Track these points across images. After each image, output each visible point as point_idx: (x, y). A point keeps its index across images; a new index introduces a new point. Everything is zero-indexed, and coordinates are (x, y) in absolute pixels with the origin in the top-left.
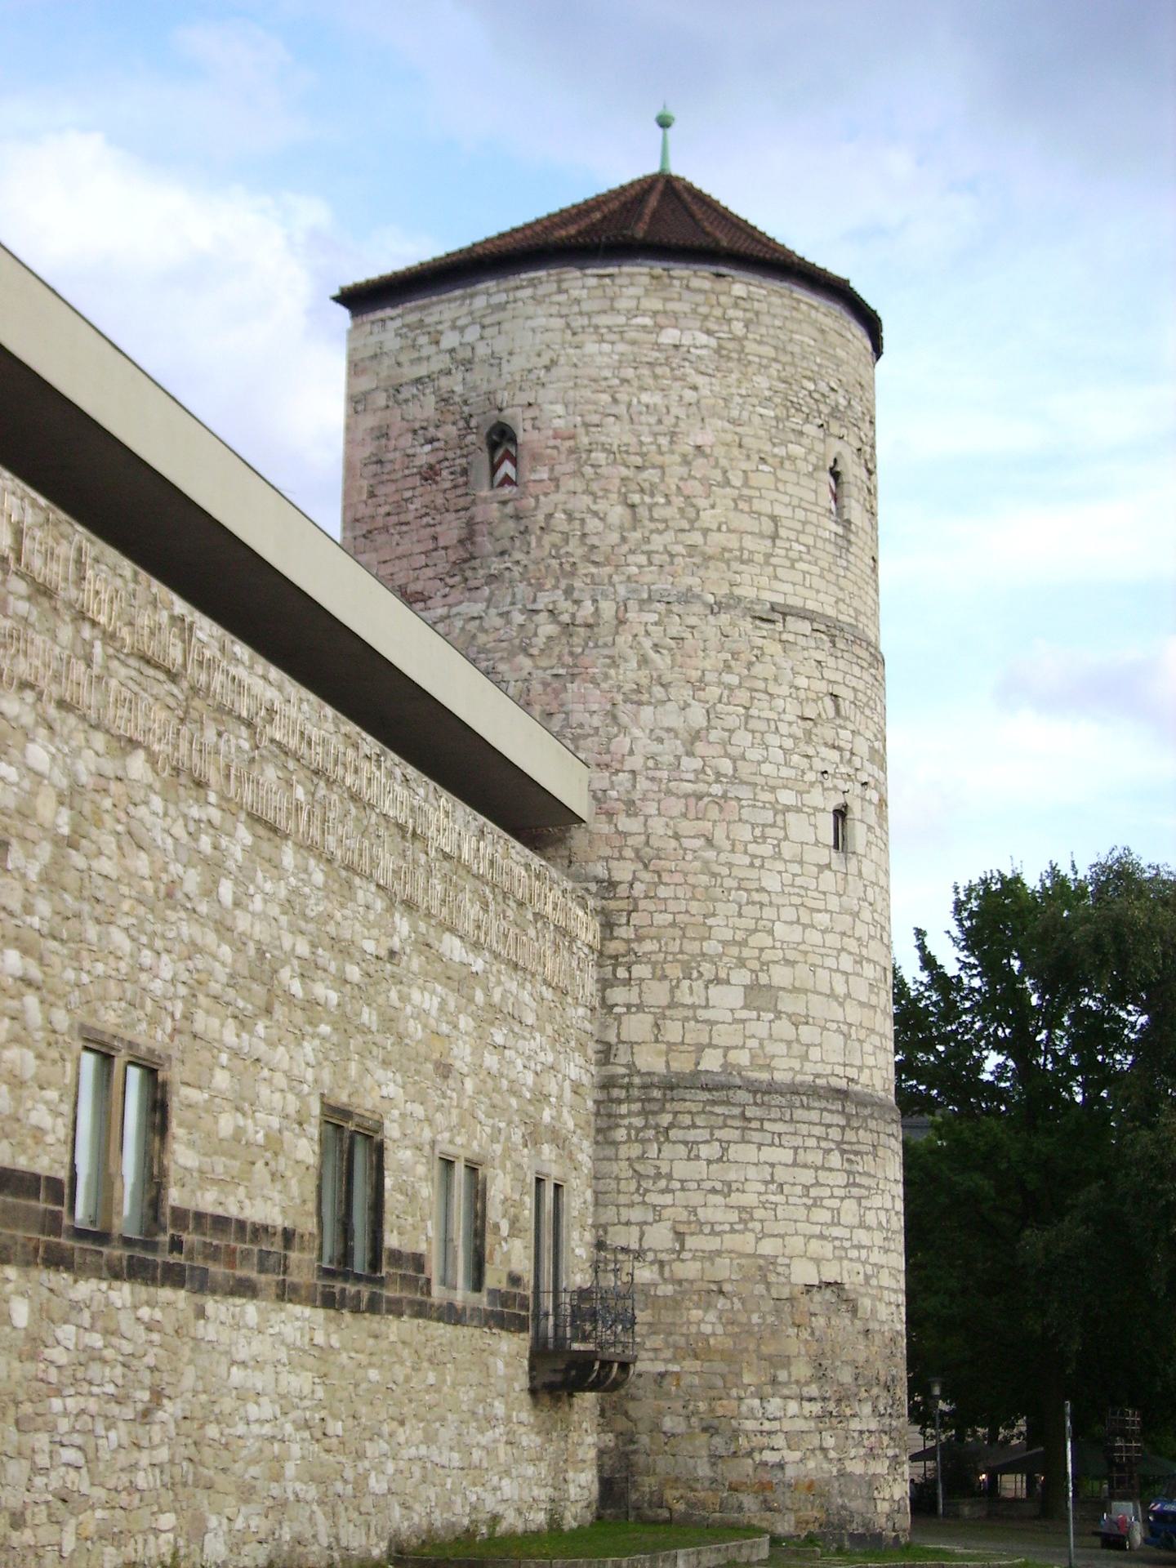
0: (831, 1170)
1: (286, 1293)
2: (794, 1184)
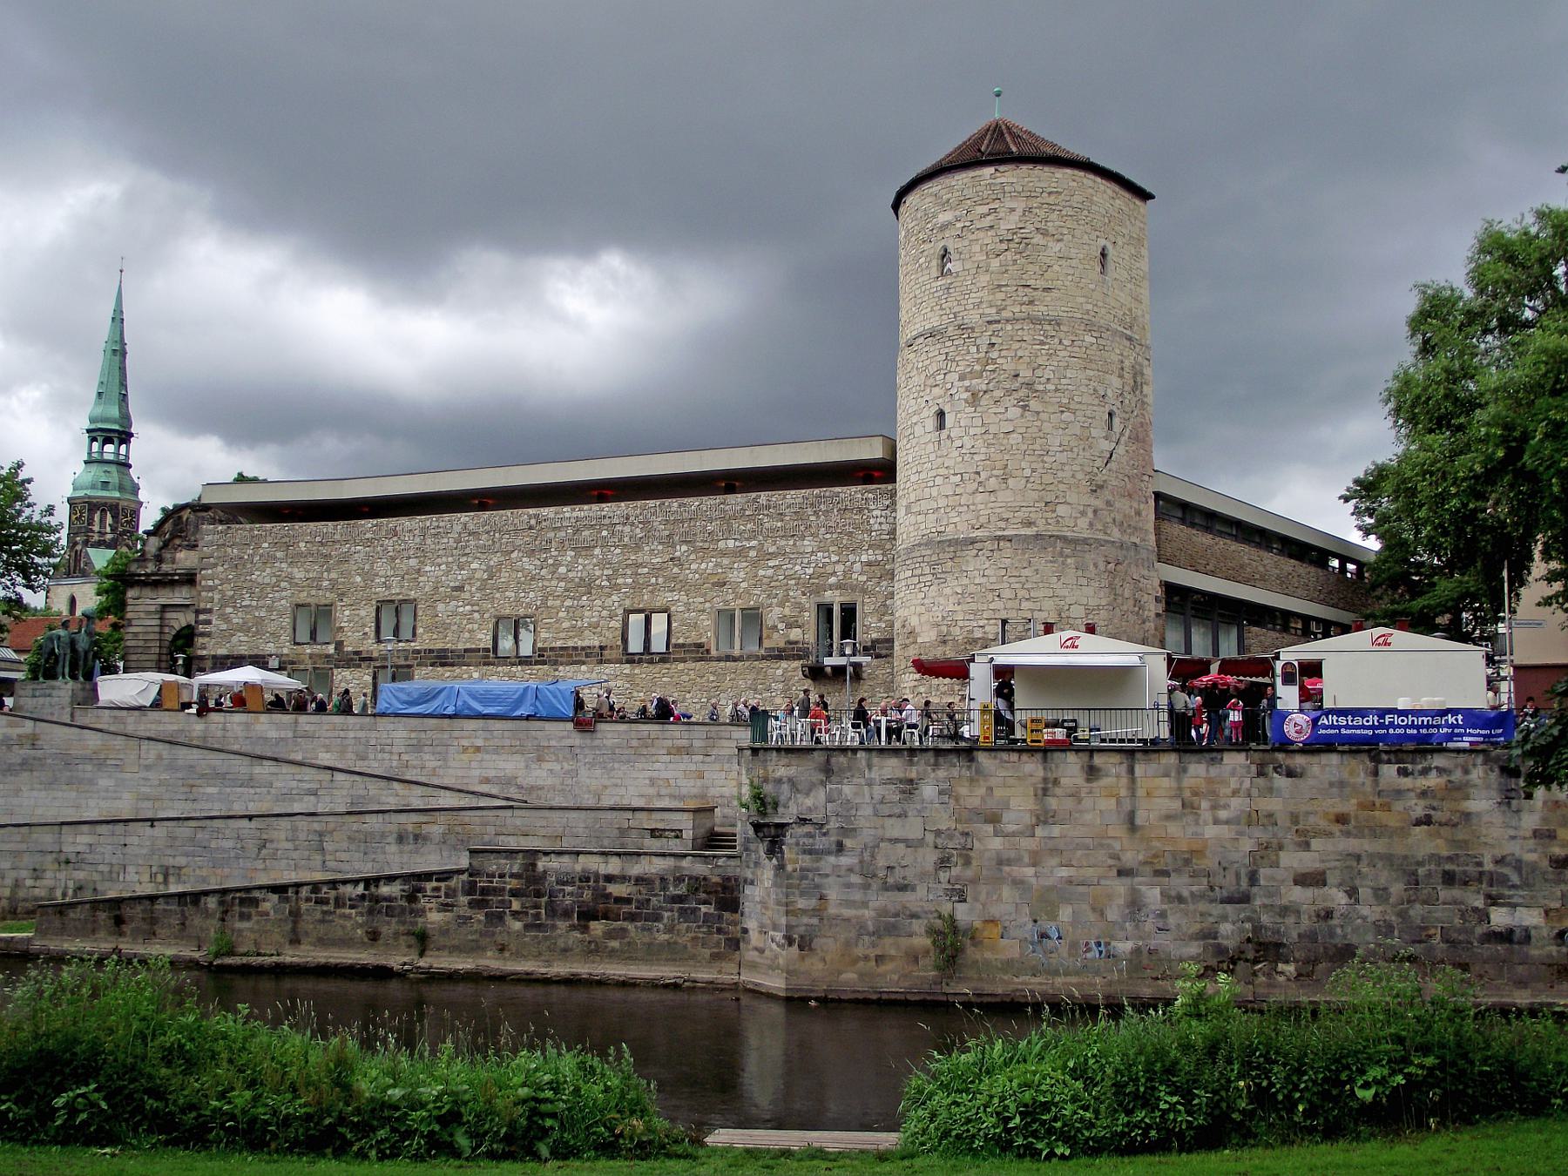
1: (601, 662)
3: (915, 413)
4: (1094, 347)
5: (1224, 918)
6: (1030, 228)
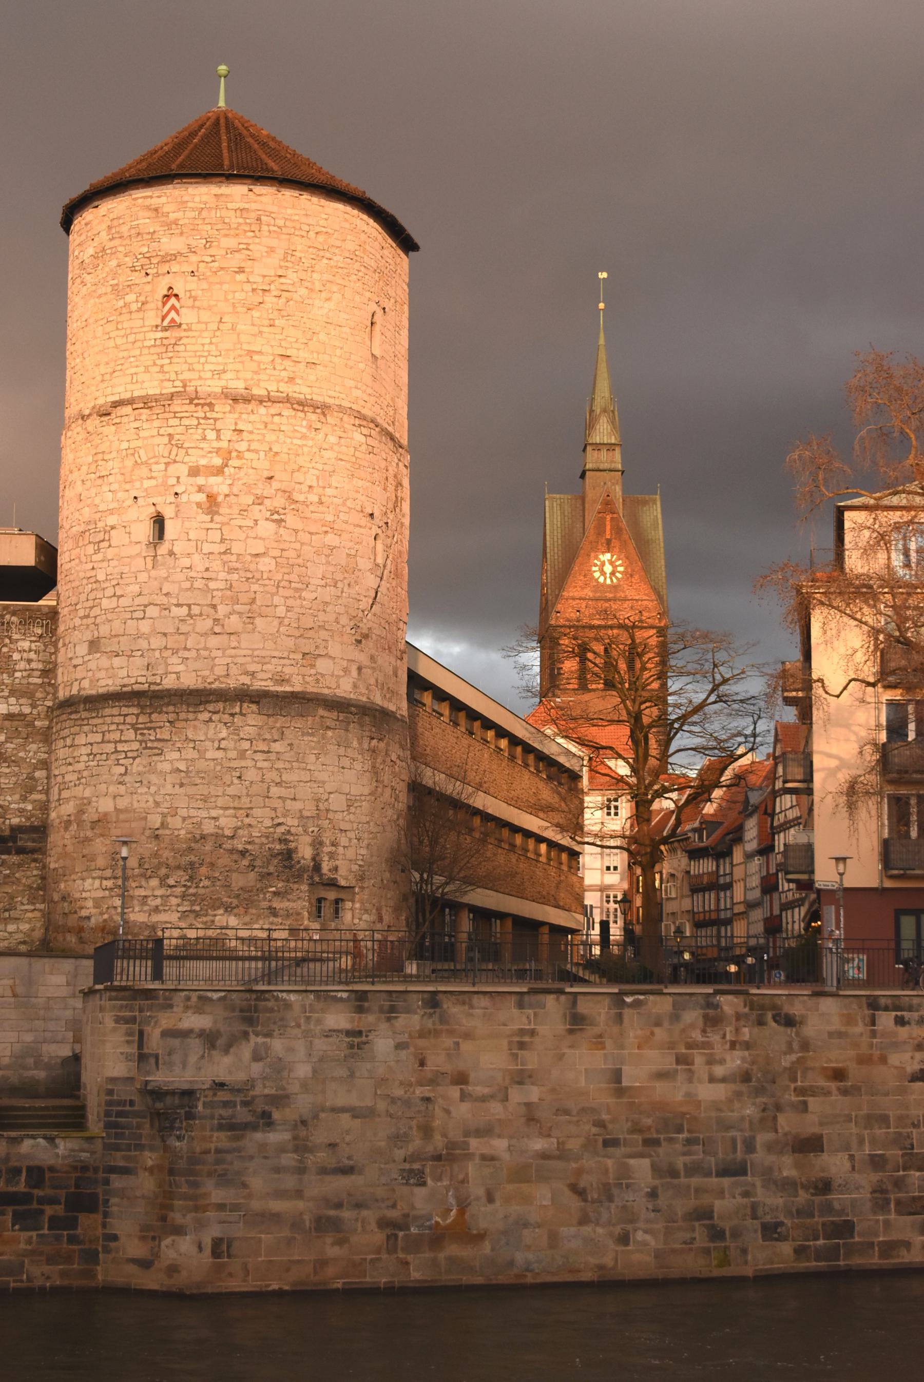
0: (126, 741)
2: (101, 754)
3: (111, 512)
4: (364, 447)
5: (721, 1194)
6: (292, 276)
